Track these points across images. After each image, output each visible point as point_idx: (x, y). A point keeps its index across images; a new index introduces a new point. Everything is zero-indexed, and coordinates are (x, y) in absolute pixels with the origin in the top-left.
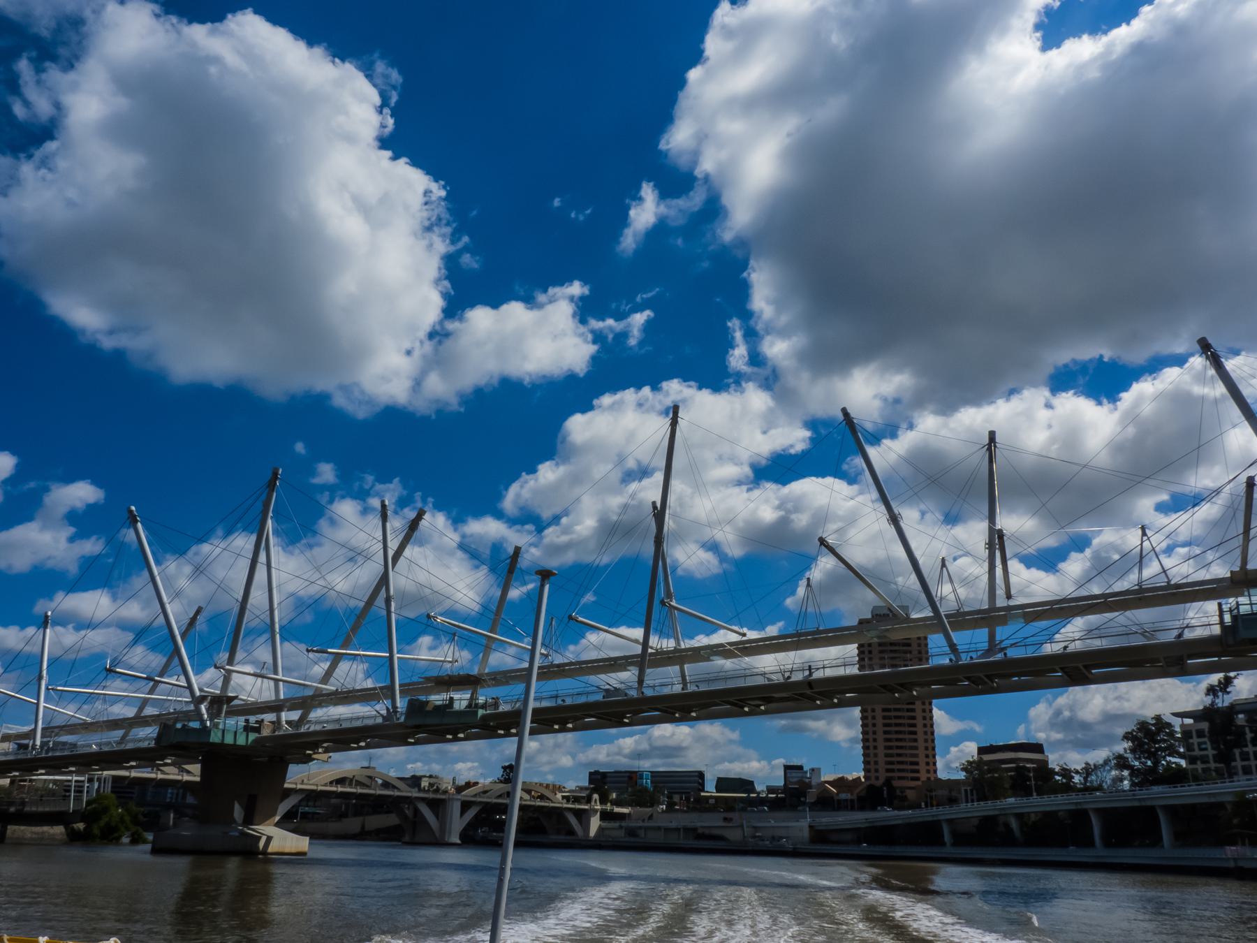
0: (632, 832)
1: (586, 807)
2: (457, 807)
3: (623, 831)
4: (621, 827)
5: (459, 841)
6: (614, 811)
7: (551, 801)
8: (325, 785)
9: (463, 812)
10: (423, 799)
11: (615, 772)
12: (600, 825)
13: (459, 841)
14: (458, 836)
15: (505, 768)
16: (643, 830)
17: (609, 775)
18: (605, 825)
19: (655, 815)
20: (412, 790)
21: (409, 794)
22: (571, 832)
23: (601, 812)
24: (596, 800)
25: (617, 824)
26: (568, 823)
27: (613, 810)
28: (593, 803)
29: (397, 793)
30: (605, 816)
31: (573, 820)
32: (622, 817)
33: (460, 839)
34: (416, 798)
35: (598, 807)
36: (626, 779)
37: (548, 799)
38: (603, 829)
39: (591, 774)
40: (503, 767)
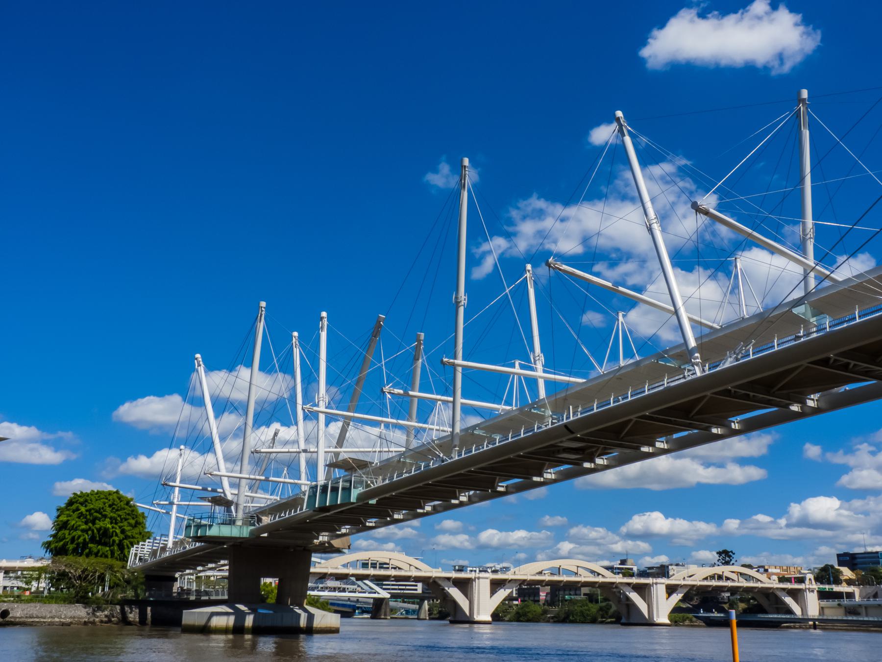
0: (852, 610)
4: (839, 605)
5: (667, 621)
6: (834, 590)
7: (761, 581)
13: (667, 621)
14: (667, 617)
16: (864, 609)
17: (857, 556)
18: (824, 603)
22: (790, 611)
23: (818, 591)
25: (836, 602)
26: (784, 603)
27: (832, 589)
28: (807, 582)
30: (823, 595)
31: (789, 600)
32: (839, 595)
34: (620, 583)
35: (815, 586)
37: (759, 580)
40: (720, 553)
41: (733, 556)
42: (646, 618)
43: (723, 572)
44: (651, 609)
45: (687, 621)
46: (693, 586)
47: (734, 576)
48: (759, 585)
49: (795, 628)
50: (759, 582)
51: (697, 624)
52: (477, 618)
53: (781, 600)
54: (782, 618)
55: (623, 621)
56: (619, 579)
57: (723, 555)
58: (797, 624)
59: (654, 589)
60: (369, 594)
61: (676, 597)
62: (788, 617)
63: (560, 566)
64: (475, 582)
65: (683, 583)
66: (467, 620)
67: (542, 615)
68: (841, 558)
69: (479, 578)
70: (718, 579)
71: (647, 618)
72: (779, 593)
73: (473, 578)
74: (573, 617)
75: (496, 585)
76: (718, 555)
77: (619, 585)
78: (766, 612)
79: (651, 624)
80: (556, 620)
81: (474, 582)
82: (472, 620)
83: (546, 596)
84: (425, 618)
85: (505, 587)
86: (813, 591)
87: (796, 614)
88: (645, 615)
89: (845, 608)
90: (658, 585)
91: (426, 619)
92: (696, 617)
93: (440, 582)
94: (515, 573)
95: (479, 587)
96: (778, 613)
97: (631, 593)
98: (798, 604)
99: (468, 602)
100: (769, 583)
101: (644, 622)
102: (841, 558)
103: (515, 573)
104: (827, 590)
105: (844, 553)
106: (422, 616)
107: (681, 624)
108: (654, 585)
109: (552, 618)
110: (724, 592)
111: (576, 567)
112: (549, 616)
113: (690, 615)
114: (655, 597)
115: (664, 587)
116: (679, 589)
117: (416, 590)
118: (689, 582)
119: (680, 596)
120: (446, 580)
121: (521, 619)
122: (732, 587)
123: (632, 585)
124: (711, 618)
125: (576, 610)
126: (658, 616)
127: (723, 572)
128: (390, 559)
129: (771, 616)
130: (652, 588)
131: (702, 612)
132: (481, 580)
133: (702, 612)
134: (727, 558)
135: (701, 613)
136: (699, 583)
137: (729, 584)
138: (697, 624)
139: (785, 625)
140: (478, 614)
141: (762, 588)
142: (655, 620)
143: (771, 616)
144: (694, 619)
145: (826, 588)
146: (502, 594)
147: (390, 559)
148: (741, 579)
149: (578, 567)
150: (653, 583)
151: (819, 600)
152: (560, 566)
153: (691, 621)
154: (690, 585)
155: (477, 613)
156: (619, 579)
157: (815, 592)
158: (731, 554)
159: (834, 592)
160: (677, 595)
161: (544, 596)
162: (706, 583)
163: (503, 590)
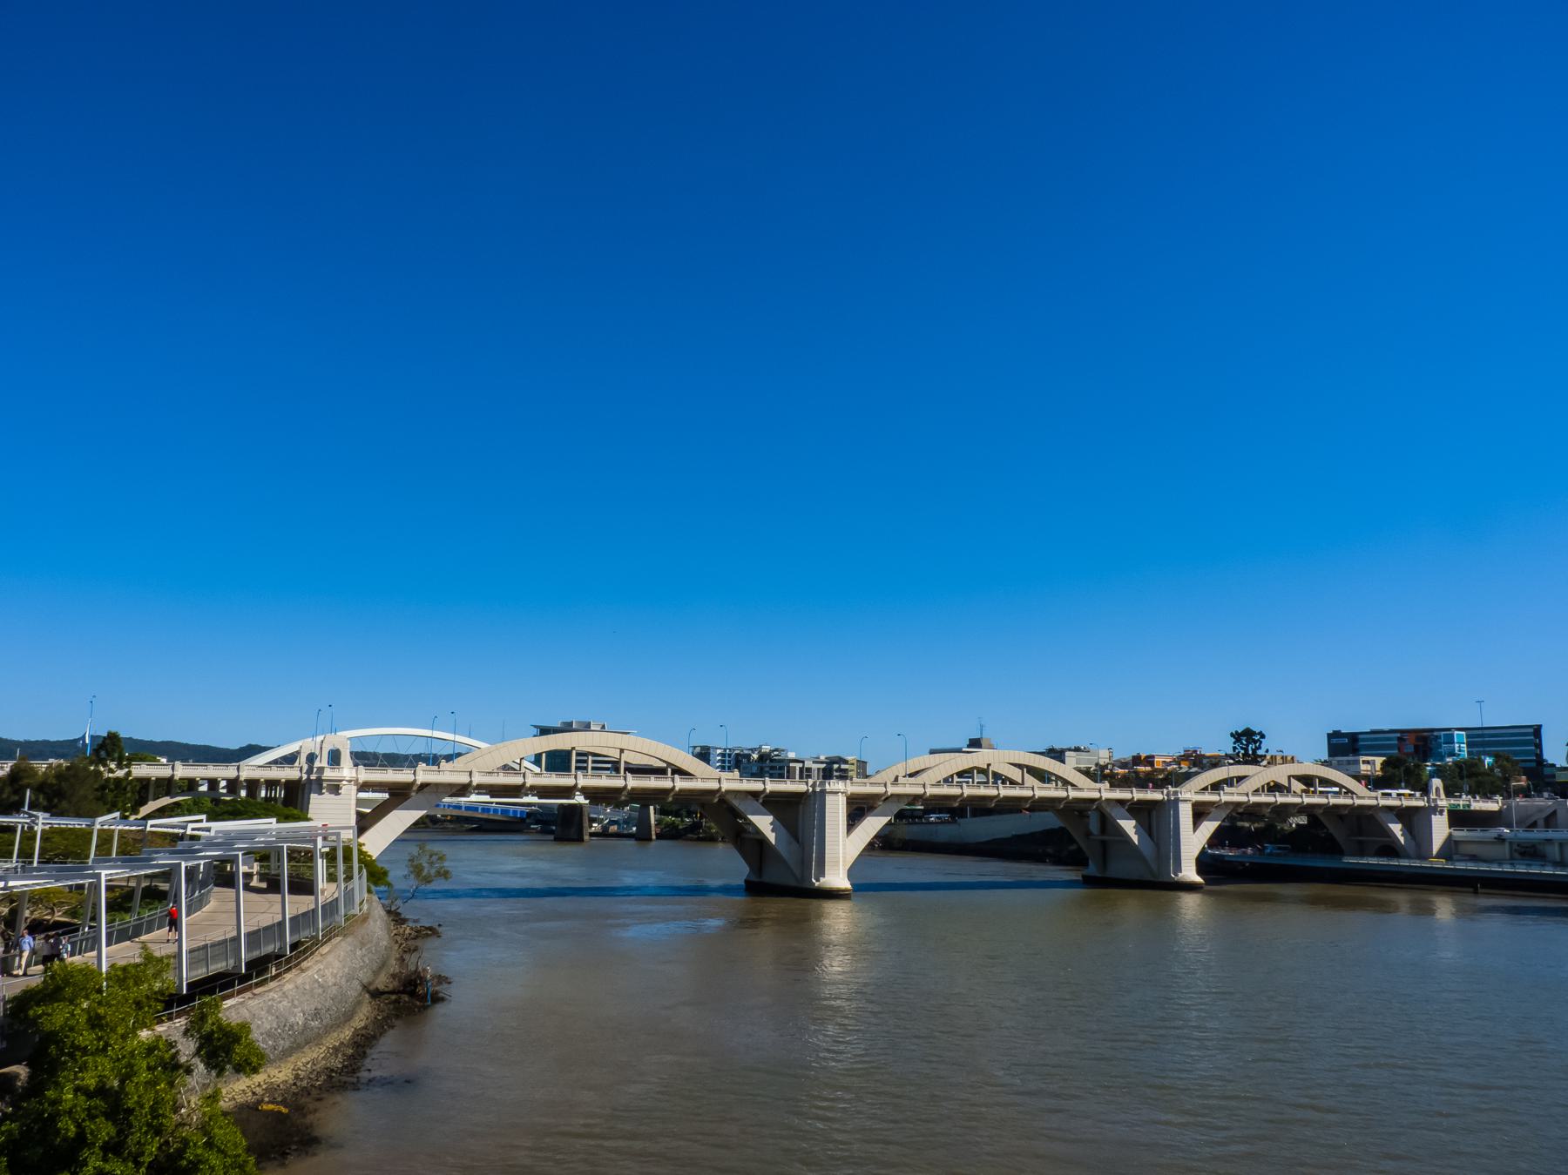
1: (1421, 803)
2: (1186, 813)
3: (1507, 846)
6: (1472, 808)
8: (938, 784)
10: (1121, 802)
11: (1373, 732)
12: (1450, 835)
15: (1237, 737)
17: (1361, 736)
18: (1461, 834)
19: (1559, 812)
20: (1098, 785)
21: (1095, 795)
23: (1448, 810)
24: (1437, 789)
27: (1469, 806)
28: (1433, 796)
29: (1073, 794)
30: (1458, 818)
33: (1199, 872)
34: (1108, 800)
35: (1443, 802)
36: (1396, 742)
38: (1456, 842)
39: (1330, 736)
40: (1232, 735)
46: (1239, 804)
56: (1106, 792)
62: (1383, 861)
66: (793, 883)
68: (1334, 741)
70: (1268, 791)
75: (858, 809)
76: (1233, 740)
77: (1103, 805)
82: (806, 885)
86: (1441, 813)
89: (1511, 843)
93: (736, 803)
94: (896, 779)
100: (1370, 798)
102: (1334, 741)
103: (896, 779)
104: (1461, 808)
105: (1334, 731)
118: (1229, 796)
120: (750, 797)
124: (1226, 859)
128: (622, 751)
145: (1459, 805)
147: (622, 751)
151: (1450, 828)
152: (989, 765)
154: (1232, 803)
156: (1106, 792)
157: (1445, 813)
159: (1472, 811)
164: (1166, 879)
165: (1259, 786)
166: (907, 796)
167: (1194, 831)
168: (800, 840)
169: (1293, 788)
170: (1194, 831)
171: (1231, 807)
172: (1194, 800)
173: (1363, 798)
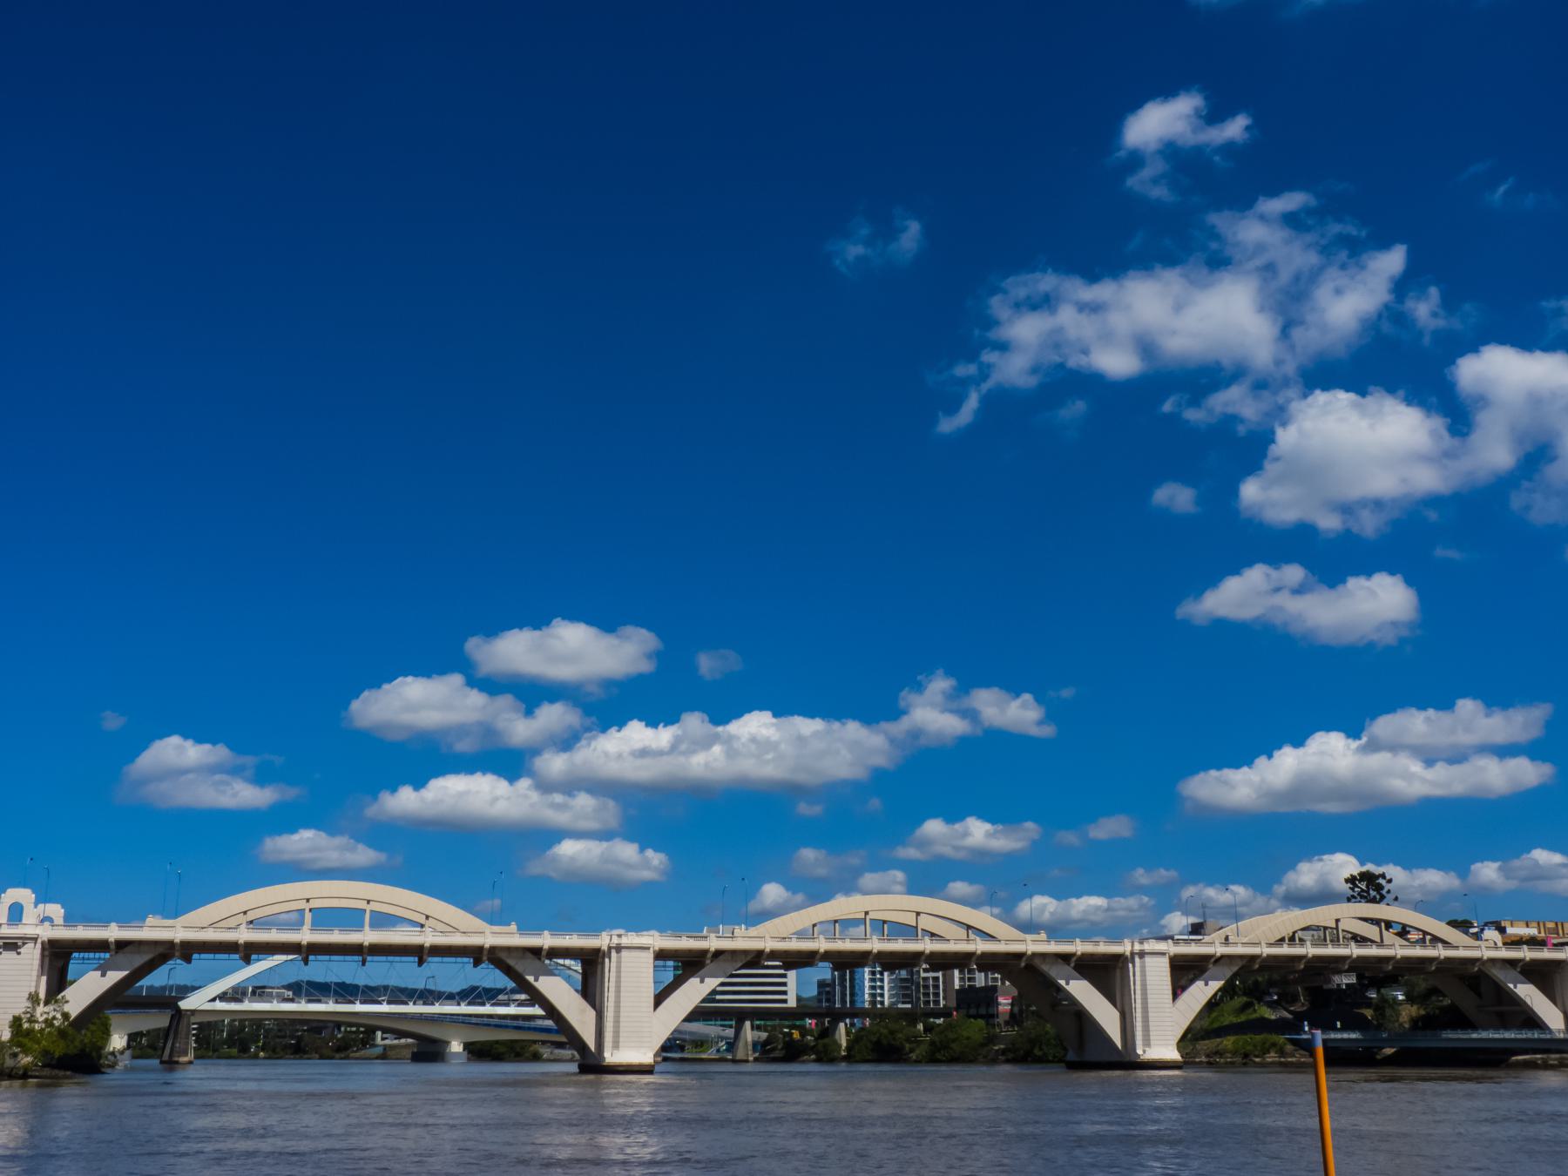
5: (1173, 1054)
9: (1178, 989)
10: (1065, 958)
13: (1173, 1054)
22: (1533, 1021)
41: (1387, 887)
42: (1118, 1048)
43: (1337, 921)
44: (1128, 1020)
45: (1272, 1054)
46: (1252, 958)
47: (1371, 931)
48: (1441, 952)
49: (1546, 1066)
50: (1440, 945)
51: (1294, 1059)
52: (611, 1057)
53: (1507, 993)
54: (1504, 1040)
55: (1071, 1056)
57: (1363, 886)
58: (1553, 1056)
59: (1135, 970)
60: (492, 1008)
61: (1201, 992)
63: (867, 913)
64: (610, 958)
65: (1220, 950)
67: (983, 1045)
69: (619, 949)
71: (1119, 1046)
72: (1499, 974)
73: (605, 948)
74: (1041, 1049)
76: (1349, 885)
78: (1470, 1025)
79: (1128, 1062)
80: (1010, 1056)
81: (607, 960)
83: (1012, 1005)
84: (745, 1058)
85: (702, 972)
87: (1548, 1028)
88: (1115, 1041)
90: (1148, 959)
91: (747, 1061)
92: (1295, 1042)
95: (619, 971)
96: (1506, 1026)
97: (1071, 982)
98: (1555, 1002)
99: (592, 1013)
101: (1115, 1058)
106: (740, 1055)
107: (1257, 1060)
108: (1137, 960)
109: (1004, 1052)
110: (1339, 972)
111: (915, 914)
112: (996, 1048)
113: (1281, 1039)
114: (1138, 992)
115: (1164, 963)
116: (1212, 970)
117: (785, 1001)
119: (1216, 985)
120: (530, 955)
121: (938, 1056)
122: (1361, 959)
123: (1074, 959)
125: (1047, 1033)
126: (1147, 1043)
127: (1337, 921)
129: (1484, 1035)
130: (1130, 965)
131: (1307, 1029)
132: (624, 953)
133: (1307, 1029)
134: (1371, 892)
135: (1305, 1032)
136: (1267, 951)
137: (1356, 951)
138: (1294, 1059)
139: (1520, 1057)
140: (616, 1045)
141: (1448, 960)
142: (1139, 1052)
143: (1484, 1035)
144: (1289, 1047)
146: (694, 992)
148: (1389, 937)
149: (918, 914)
150: (1132, 954)
153: (1282, 1053)
154: (1241, 957)
155: (614, 1042)
158: (1381, 881)
160: (1206, 984)
161: (1008, 1004)
162: (1285, 950)
163: (698, 980)
164: (1133, 1059)
165: (1287, 932)
166: (745, 952)
167: (1175, 996)
168: (597, 1007)
169: (1386, 942)
170: (1175, 996)
171: (1244, 962)
172: (1172, 954)
173: (1457, 947)
